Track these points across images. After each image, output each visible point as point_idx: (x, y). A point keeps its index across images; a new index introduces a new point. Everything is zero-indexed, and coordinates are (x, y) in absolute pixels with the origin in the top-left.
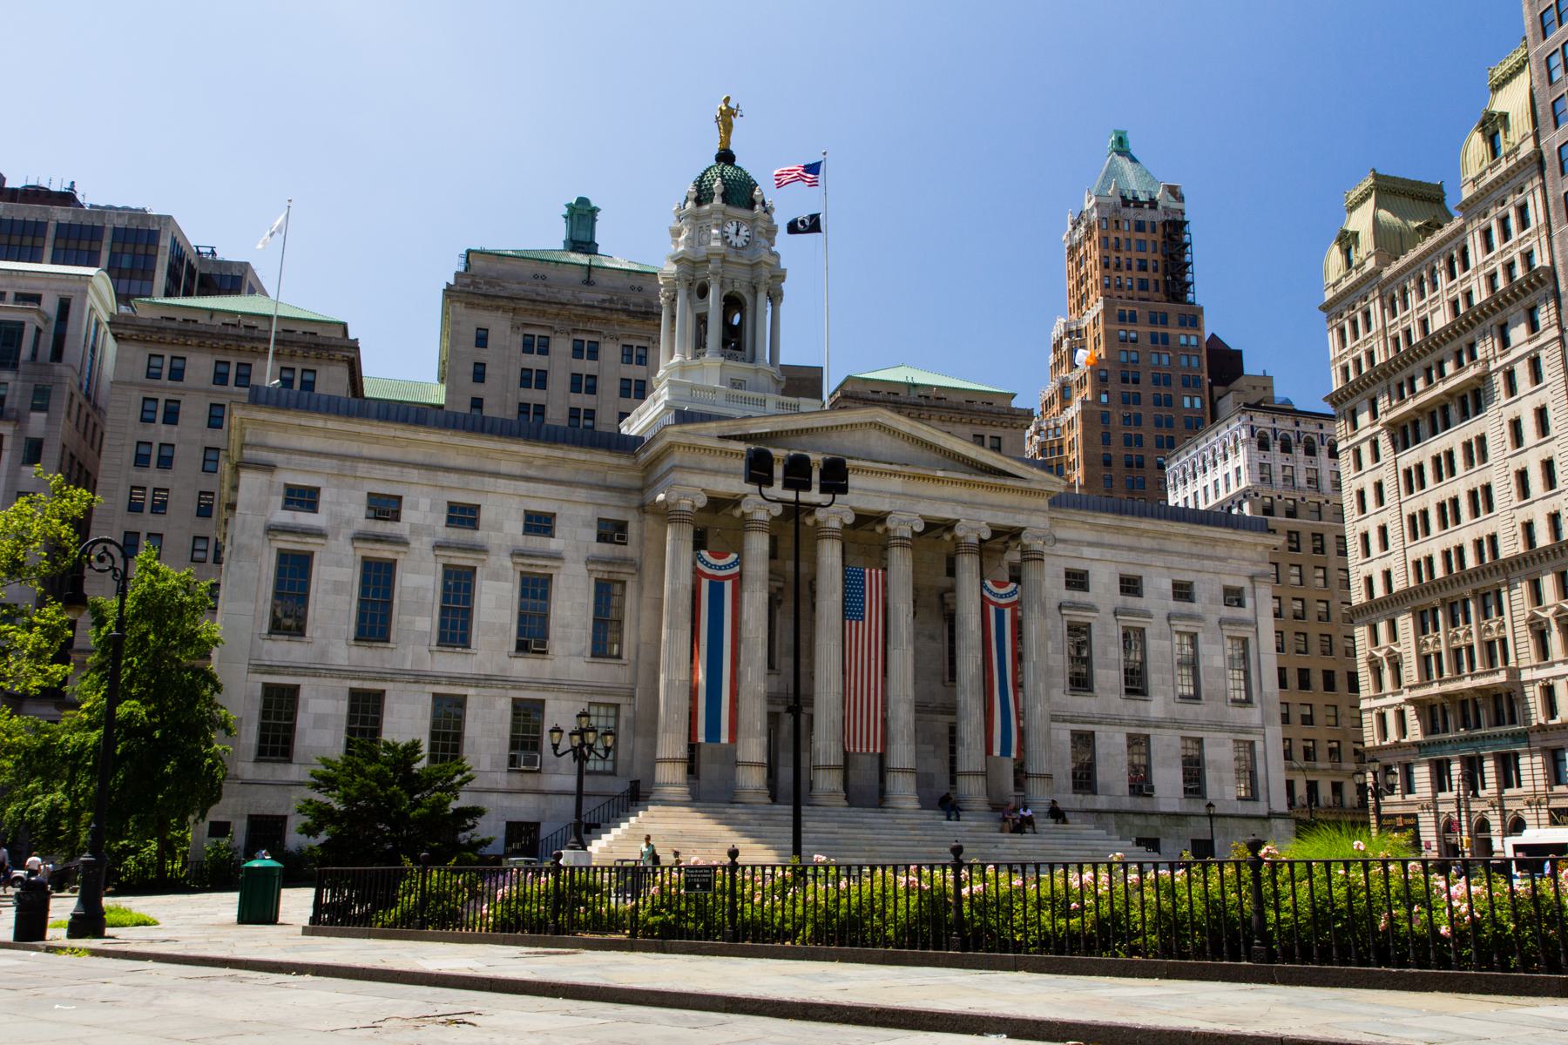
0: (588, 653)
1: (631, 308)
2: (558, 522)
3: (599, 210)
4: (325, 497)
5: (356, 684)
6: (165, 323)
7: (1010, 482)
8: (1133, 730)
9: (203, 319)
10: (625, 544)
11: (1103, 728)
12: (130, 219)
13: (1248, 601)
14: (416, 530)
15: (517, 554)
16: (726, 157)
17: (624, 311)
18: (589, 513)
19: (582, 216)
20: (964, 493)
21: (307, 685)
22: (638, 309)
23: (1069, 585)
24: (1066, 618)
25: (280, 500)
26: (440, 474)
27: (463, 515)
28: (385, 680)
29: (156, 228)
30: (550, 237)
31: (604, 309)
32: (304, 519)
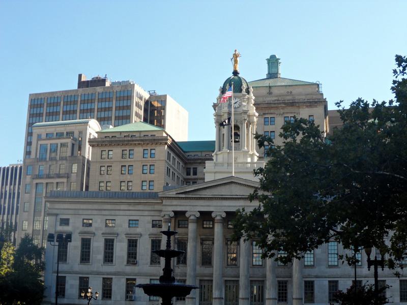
0: (149, 264)
1: (286, 101)
2: (139, 222)
3: (279, 59)
4: (71, 221)
5: (81, 276)
6: (105, 139)
9: (118, 135)
10: (161, 227)
11: (342, 279)
12: (121, 88)
14: (97, 229)
16: (235, 73)
17: (283, 103)
18: (150, 219)
19: (273, 62)
22: (289, 101)
25: (58, 223)
26: (103, 211)
29: (130, 89)
31: (275, 104)
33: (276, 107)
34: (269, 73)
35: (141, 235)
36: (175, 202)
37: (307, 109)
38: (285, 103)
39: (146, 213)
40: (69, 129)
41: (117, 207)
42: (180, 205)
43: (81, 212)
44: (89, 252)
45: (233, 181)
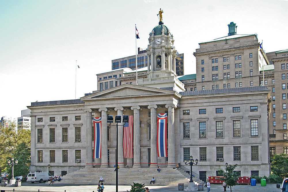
17: (233, 48)
19: (232, 26)
20: (150, 99)
30: (223, 33)
33: (230, 51)
34: (229, 33)
36: (92, 103)
37: (248, 50)
38: (235, 48)
40: (114, 74)
41: (68, 109)
42: (95, 105)
43: (48, 114)
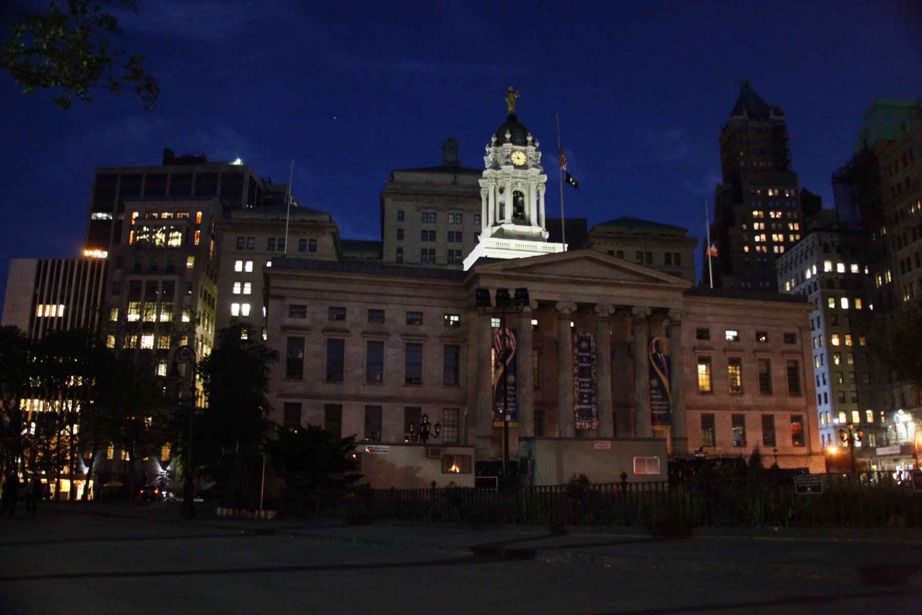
7: (661, 284)
8: (735, 412)
13: (798, 341)
15: (404, 335)
21: (306, 403)
23: (699, 337)
24: (697, 355)
25: (287, 313)
27: (376, 316)
28: (340, 399)
32: (300, 322)
35: (427, 336)
39: (435, 302)
44: (342, 361)
45: (589, 255)
